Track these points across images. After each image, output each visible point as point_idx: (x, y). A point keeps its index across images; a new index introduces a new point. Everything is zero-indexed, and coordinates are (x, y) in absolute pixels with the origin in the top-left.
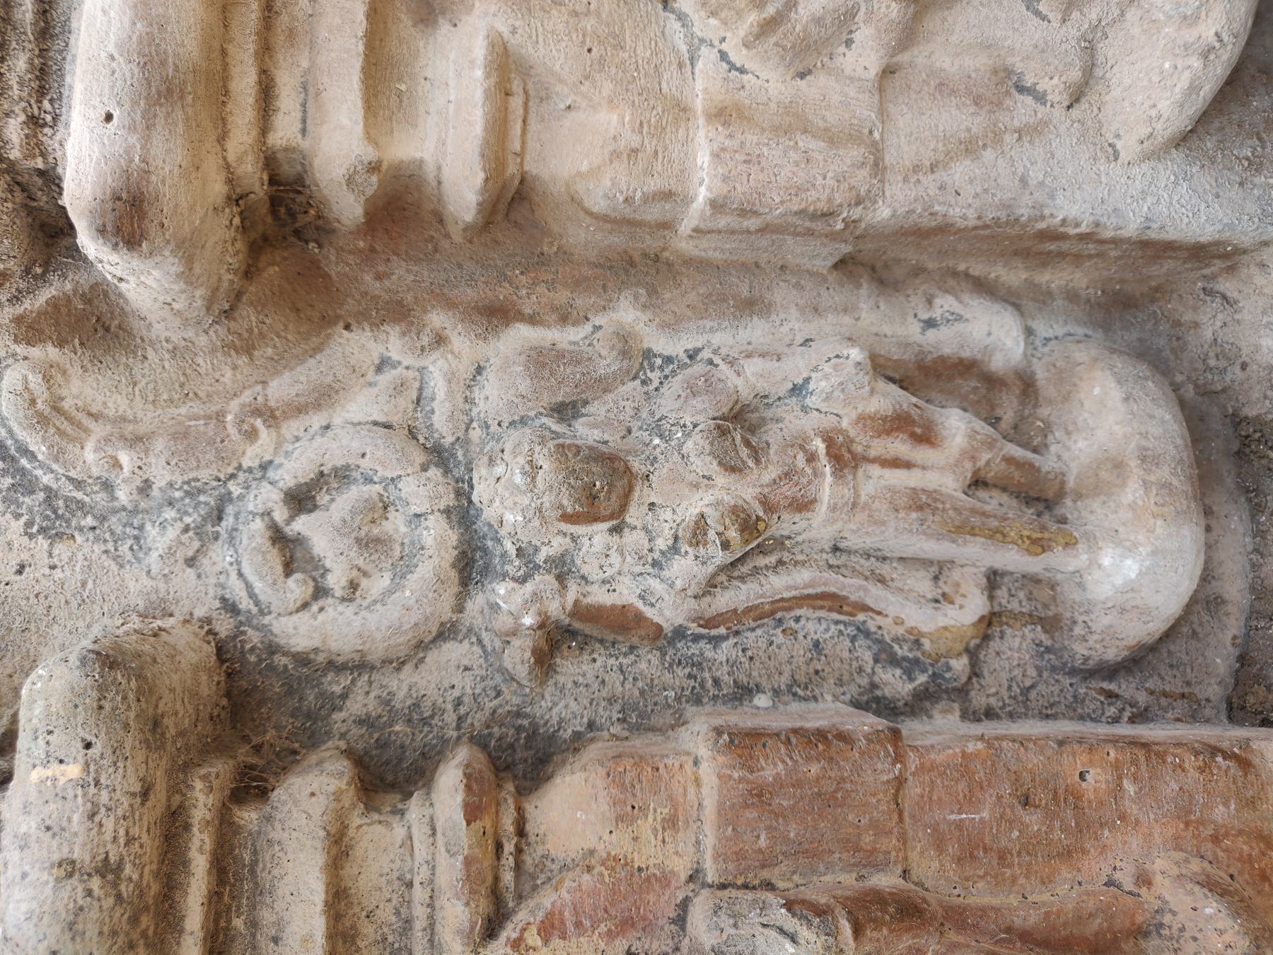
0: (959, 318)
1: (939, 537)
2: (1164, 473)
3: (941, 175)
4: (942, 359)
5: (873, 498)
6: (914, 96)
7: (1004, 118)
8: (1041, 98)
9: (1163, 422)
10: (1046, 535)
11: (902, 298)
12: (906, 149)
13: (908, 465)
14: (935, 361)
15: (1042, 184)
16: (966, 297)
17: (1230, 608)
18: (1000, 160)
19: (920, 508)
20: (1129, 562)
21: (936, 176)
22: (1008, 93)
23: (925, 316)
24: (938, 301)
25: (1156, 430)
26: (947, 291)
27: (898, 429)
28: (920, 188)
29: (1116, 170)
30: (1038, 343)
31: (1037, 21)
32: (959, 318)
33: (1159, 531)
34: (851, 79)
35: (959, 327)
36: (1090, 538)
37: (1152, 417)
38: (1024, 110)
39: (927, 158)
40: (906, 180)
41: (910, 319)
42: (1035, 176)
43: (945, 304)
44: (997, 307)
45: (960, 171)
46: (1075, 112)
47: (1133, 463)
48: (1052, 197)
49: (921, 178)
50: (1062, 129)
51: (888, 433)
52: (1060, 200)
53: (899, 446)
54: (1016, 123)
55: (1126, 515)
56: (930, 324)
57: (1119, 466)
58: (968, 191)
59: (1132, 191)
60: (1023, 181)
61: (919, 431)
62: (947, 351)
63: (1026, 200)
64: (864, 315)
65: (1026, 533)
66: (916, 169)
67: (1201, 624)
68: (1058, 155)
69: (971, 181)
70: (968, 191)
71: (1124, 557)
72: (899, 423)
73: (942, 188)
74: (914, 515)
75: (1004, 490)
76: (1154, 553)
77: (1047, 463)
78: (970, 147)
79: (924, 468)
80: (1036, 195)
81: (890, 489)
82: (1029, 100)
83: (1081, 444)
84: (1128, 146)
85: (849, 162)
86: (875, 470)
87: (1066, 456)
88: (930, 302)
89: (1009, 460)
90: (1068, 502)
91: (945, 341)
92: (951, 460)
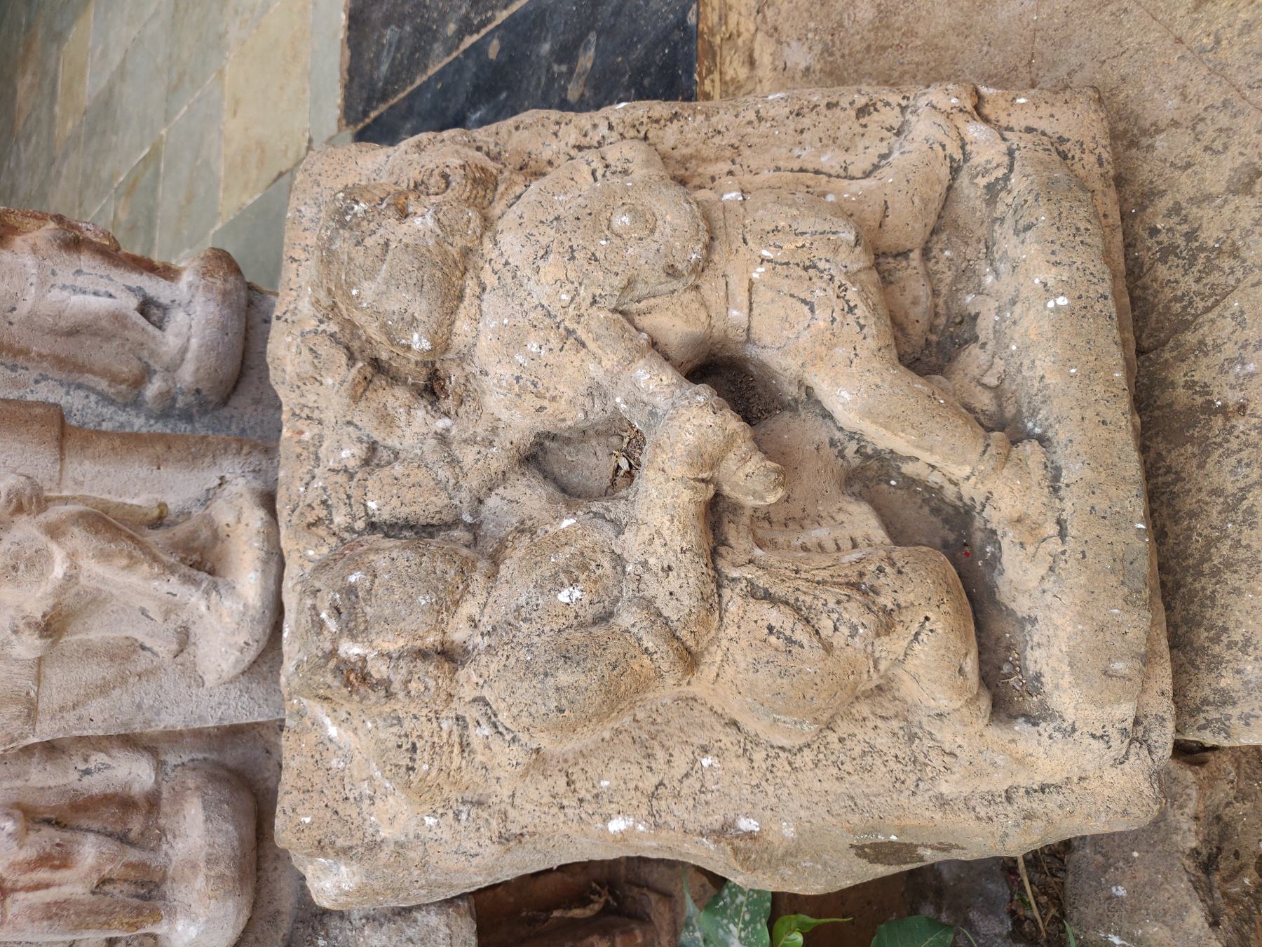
0: (108, 767)
1: (63, 933)
2: (221, 868)
3: (81, 711)
4: (91, 797)
5: (16, 916)
6: (66, 660)
7: (130, 666)
8: (155, 654)
9: (227, 832)
10: (140, 919)
11: (66, 758)
12: (55, 696)
13: (47, 886)
14: (85, 800)
15: (152, 707)
16: (115, 752)
17: (284, 916)
18: (125, 696)
19: (50, 918)
20: (192, 928)
21: (77, 712)
22: (135, 651)
23: (84, 768)
24: (93, 758)
25: (220, 840)
26: (101, 751)
27: (41, 866)
28: (63, 722)
29: (202, 691)
30: (169, 770)
31: (148, 621)
32: (108, 767)
33: (212, 907)
34: (16, 660)
35: (107, 773)
36: (172, 912)
37: (219, 831)
38: (143, 661)
39: (70, 699)
40: (53, 718)
41: (71, 771)
42: (148, 702)
43: (98, 758)
44: (137, 755)
45: (95, 708)
46: (179, 659)
47: (202, 864)
48: (158, 714)
49: (65, 714)
50: (170, 670)
51: (32, 870)
52: (163, 715)
53: (43, 875)
54: (139, 669)
55: (195, 895)
56: (87, 772)
57: (194, 867)
58: (98, 719)
59: (212, 704)
60: (139, 707)
61: (57, 863)
62: (95, 791)
63: (140, 718)
64: (33, 776)
65: (125, 920)
66: (62, 709)
67: (263, 932)
68: (166, 686)
69: (102, 711)
70: (98, 719)
71: (189, 925)
72: (44, 860)
73: (80, 719)
74: (45, 923)
75: (125, 881)
76: (207, 922)
77: (155, 861)
78: (104, 689)
79: (60, 885)
80: (147, 715)
81: (31, 907)
82: (148, 654)
83: (180, 845)
84: (210, 679)
85: (7, 716)
86: (21, 896)
87: (170, 852)
88: (86, 760)
89: (129, 865)
90: (169, 882)
91: (96, 784)
92: (83, 875)
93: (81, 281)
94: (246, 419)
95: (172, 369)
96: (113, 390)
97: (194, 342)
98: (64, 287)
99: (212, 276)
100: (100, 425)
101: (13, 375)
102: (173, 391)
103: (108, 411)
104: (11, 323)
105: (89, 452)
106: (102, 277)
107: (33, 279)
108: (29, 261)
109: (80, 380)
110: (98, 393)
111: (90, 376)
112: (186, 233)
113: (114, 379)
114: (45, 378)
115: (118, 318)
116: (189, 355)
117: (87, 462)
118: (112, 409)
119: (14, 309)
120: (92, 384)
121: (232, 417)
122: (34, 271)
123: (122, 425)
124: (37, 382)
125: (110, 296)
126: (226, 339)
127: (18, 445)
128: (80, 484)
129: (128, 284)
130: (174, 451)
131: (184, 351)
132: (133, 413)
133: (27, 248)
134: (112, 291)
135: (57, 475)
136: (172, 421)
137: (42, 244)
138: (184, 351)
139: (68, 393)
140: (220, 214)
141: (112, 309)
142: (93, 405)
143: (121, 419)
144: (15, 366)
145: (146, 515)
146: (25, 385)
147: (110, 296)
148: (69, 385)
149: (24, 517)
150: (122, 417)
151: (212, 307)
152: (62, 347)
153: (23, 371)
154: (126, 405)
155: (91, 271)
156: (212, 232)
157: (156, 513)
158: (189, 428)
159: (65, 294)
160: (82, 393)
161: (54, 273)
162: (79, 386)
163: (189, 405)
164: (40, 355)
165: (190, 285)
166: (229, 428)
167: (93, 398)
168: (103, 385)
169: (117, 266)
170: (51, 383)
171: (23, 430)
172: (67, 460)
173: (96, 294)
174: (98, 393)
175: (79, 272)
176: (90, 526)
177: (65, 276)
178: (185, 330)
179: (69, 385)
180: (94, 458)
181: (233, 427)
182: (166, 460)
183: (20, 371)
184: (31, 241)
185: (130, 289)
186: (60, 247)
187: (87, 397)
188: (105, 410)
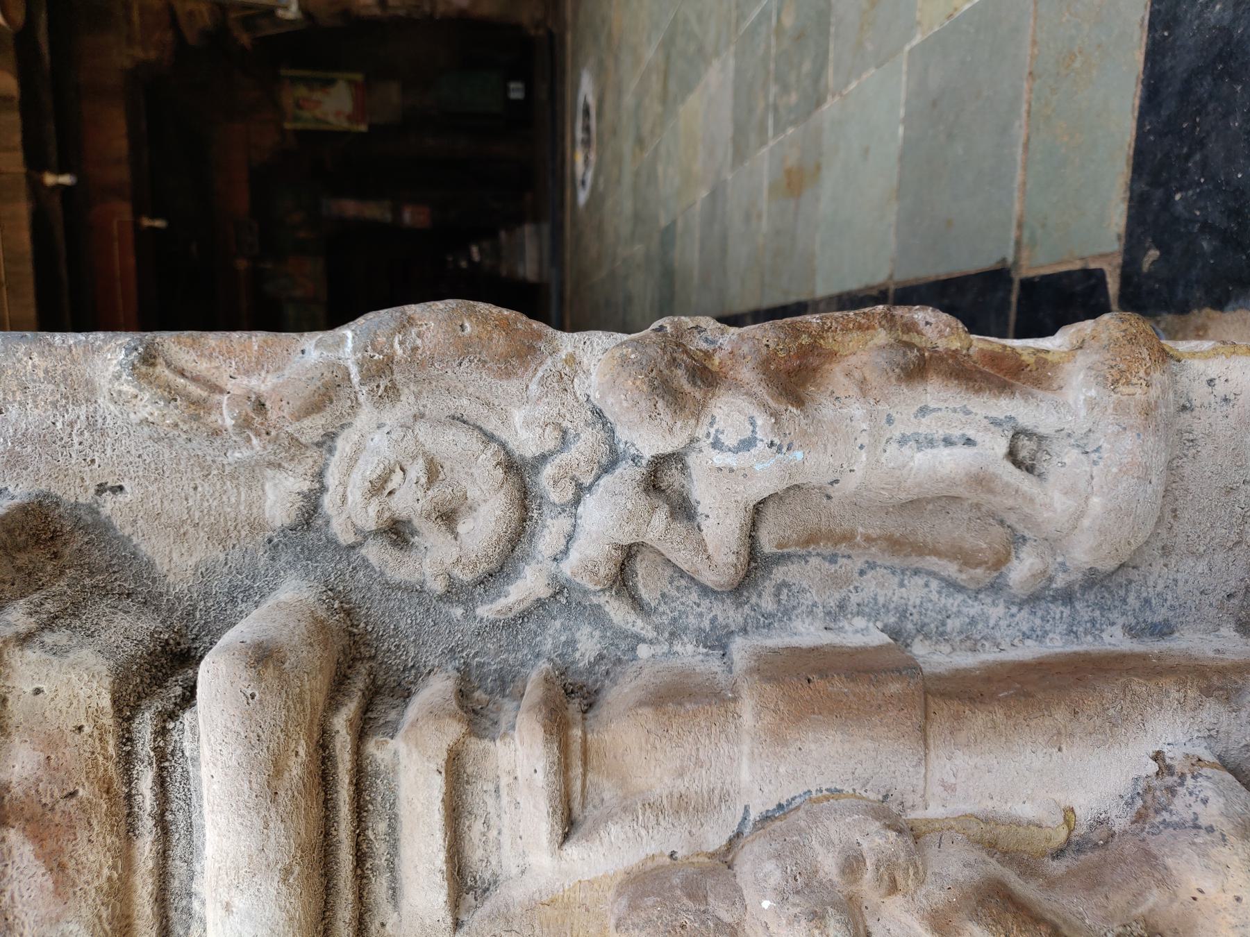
93: (926, 426)
94: (1151, 583)
95: (1053, 544)
96: (964, 576)
97: (1096, 501)
98: (903, 441)
99: (1128, 383)
100: (944, 624)
101: (833, 568)
102: (1052, 568)
103: (953, 602)
104: (829, 497)
105: (962, 736)
106: (955, 411)
107: (864, 439)
108: (857, 410)
109: (919, 565)
110: (942, 579)
111: (934, 559)
112: (869, 47)
113: (966, 559)
114: (872, 566)
115: (981, 481)
116: (1086, 522)
117: (959, 753)
118: (960, 597)
119: (837, 481)
120: (936, 569)
121: (1130, 582)
122: (864, 426)
123: (973, 621)
124: (862, 573)
125: (969, 442)
126: (1150, 489)
127: (868, 744)
128: (949, 788)
129: (993, 414)
130: (1083, 719)
131: (1080, 515)
132: (989, 600)
133: (854, 391)
134: (971, 433)
135: (921, 783)
136: (1043, 605)
137: (873, 378)
138: (1080, 515)
139: (902, 585)
140: (919, 23)
141: (974, 470)
142: (934, 596)
143: (972, 612)
144: (835, 555)
145: (1048, 840)
146: (848, 581)
147: (969, 442)
148: (903, 573)
149: (898, 899)
150: (974, 609)
151: (1129, 441)
152: (894, 527)
153: (845, 561)
154: (978, 592)
155: (942, 405)
156: (907, 48)
157: (1063, 834)
158: (1067, 611)
159: (906, 450)
160: (920, 581)
161: (890, 420)
162: (916, 572)
163: (1070, 585)
164: (868, 539)
165: (1092, 404)
166: (1124, 601)
167: (934, 584)
168: (951, 569)
169: (979, 391)
170: (881, 571)
171: (875, 719)
172: (932, 755)
173: (948, 442)
174: (942, 579)
175: (924, 411)
176: (997, 922)
177: (906, 424)
178: (1082, 485)
179: (903, 573)
180: (968, 746)
181: (1131, 599)
182: (1072, 735)
183: (841, 561)
184: (857, 374)
185: (996, 422)
186: (899, 379)
187: (926, 585)
188: (951, 600)
